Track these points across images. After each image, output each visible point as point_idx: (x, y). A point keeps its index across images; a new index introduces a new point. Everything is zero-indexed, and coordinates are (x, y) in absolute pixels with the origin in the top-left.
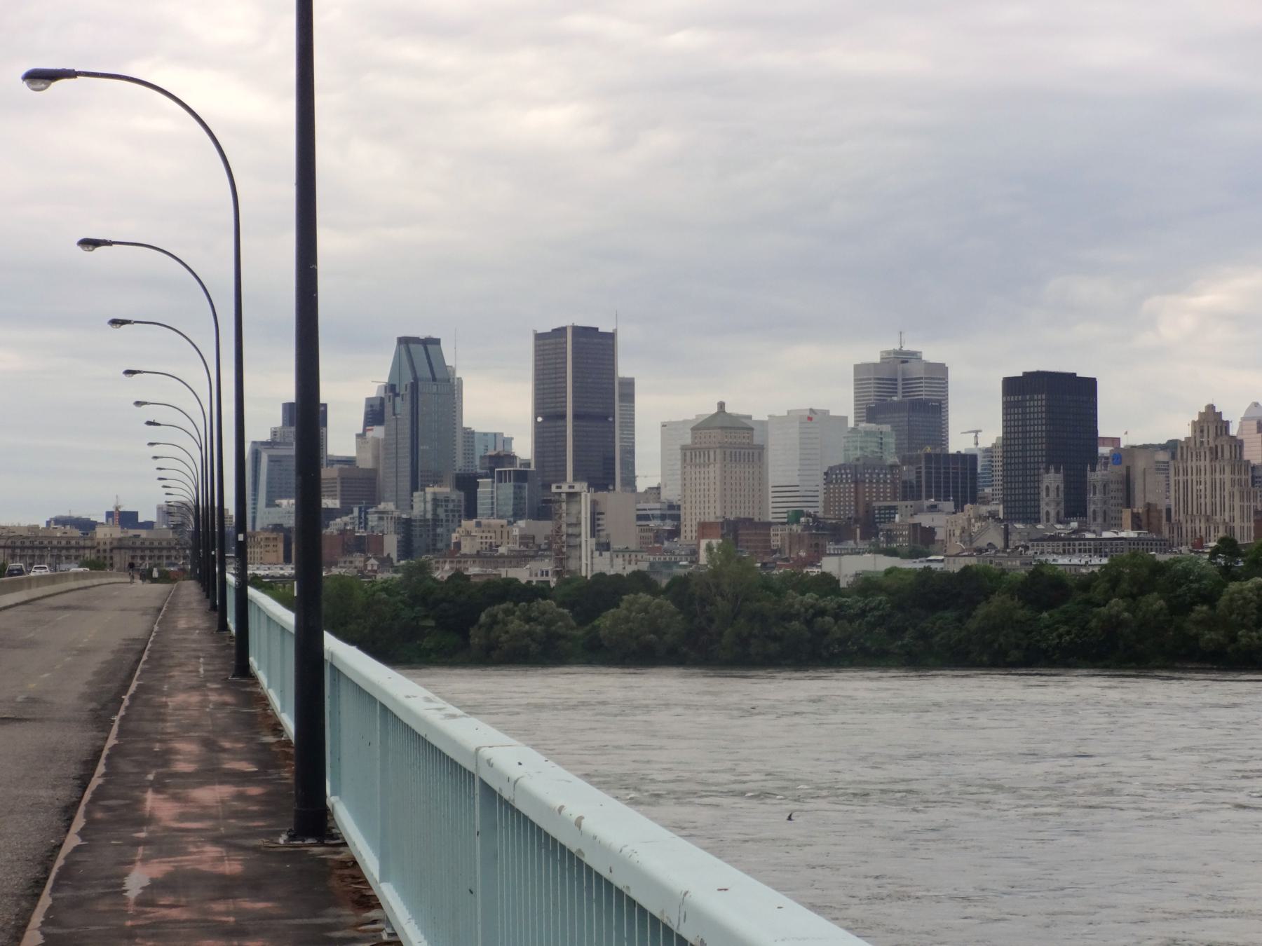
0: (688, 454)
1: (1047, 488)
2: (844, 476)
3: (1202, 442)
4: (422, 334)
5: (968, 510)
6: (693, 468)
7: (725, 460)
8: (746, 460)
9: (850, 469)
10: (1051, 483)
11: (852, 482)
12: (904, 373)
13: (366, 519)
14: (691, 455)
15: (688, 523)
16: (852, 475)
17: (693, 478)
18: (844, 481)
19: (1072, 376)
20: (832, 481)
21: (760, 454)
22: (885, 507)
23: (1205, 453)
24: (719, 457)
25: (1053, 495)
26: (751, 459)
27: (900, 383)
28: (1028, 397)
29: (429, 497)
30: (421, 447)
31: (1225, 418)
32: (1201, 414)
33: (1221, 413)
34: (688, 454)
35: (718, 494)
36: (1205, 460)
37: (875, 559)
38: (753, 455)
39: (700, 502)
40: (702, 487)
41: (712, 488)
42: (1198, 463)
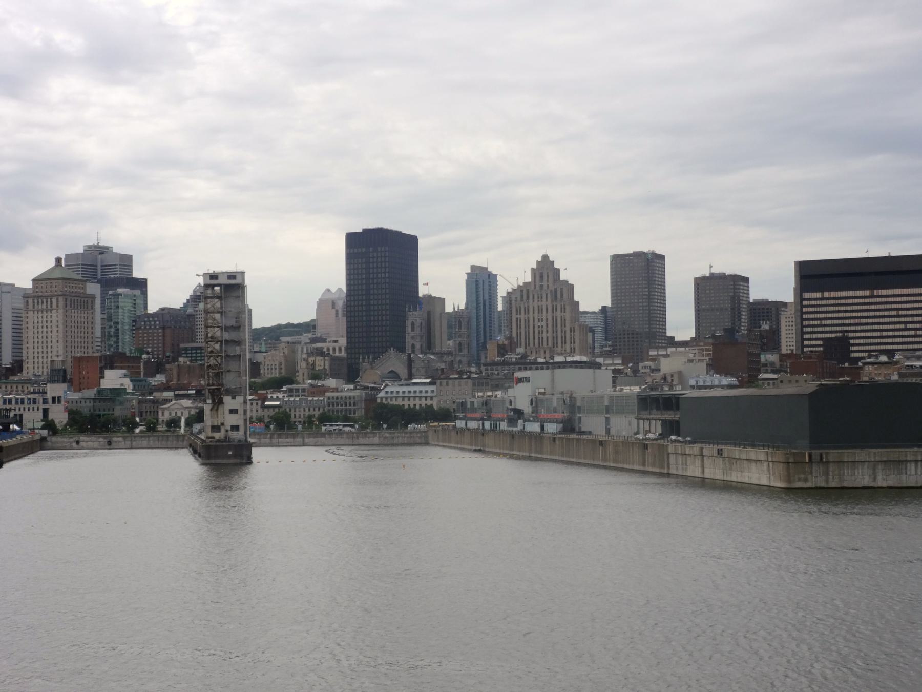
0: (31, 301)
1: (413, 324)
2: (153, 323)
3: (541, 286)
5: (283, 349)
6: (36, 313)
7: (66, 306)
8: (82, 307)
9: (158, 317)
10: (416, 320)
11: (160, 328)
12: (102, 261)
14: (34, 302)
15: (31, 360)
16: (159, 321)
17: (36, 322)
18: (152, 327)
19: (400, 233)
20: (141, 327)
21: (92, 301)
22: (191, 348)
23: (547, 295)
24: (61, 304)
25: (417, 330)
26: (86, 307)
27: (99, 268)
28: (371, 249)
31: (556, 266)
32: (538, 262)
33: (553, 262)
34: (31, 301)
35: (61, 335)
36: (547, 301)
37: (594, 372)
38: (87, 303)
39: (42, 342)
40: (45, 329)
41: (55, 329)
42: (540, 304)
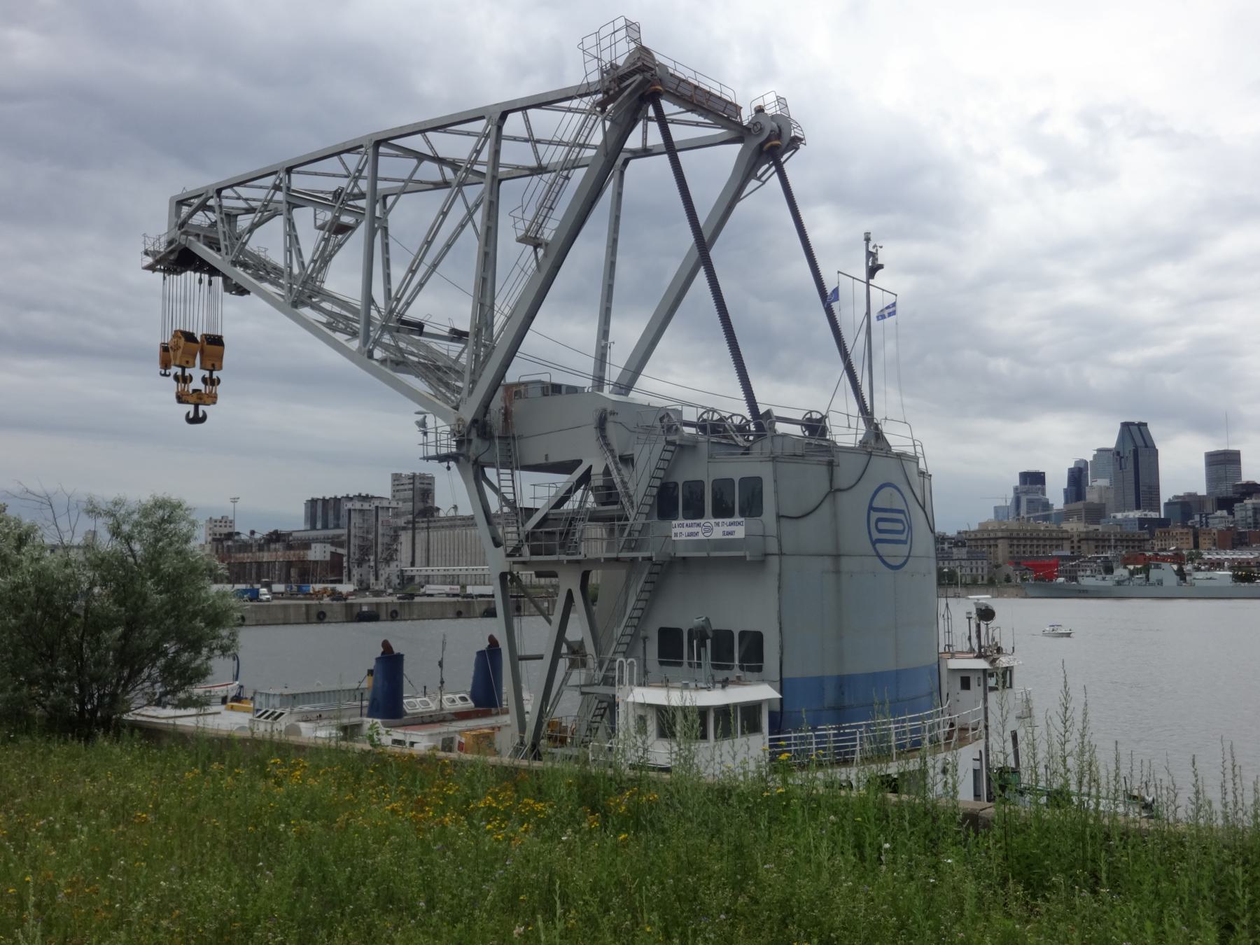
4: (1136, 420)
13: (1207, 523)
29: (1250, 506)
30: (1142, 488)
